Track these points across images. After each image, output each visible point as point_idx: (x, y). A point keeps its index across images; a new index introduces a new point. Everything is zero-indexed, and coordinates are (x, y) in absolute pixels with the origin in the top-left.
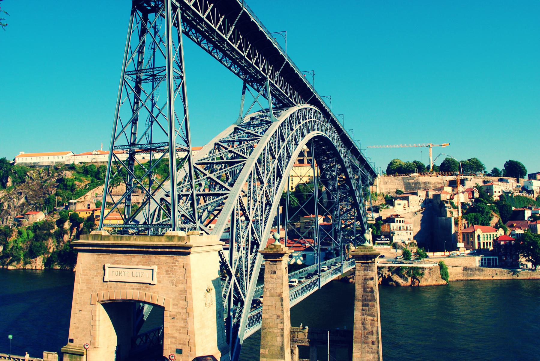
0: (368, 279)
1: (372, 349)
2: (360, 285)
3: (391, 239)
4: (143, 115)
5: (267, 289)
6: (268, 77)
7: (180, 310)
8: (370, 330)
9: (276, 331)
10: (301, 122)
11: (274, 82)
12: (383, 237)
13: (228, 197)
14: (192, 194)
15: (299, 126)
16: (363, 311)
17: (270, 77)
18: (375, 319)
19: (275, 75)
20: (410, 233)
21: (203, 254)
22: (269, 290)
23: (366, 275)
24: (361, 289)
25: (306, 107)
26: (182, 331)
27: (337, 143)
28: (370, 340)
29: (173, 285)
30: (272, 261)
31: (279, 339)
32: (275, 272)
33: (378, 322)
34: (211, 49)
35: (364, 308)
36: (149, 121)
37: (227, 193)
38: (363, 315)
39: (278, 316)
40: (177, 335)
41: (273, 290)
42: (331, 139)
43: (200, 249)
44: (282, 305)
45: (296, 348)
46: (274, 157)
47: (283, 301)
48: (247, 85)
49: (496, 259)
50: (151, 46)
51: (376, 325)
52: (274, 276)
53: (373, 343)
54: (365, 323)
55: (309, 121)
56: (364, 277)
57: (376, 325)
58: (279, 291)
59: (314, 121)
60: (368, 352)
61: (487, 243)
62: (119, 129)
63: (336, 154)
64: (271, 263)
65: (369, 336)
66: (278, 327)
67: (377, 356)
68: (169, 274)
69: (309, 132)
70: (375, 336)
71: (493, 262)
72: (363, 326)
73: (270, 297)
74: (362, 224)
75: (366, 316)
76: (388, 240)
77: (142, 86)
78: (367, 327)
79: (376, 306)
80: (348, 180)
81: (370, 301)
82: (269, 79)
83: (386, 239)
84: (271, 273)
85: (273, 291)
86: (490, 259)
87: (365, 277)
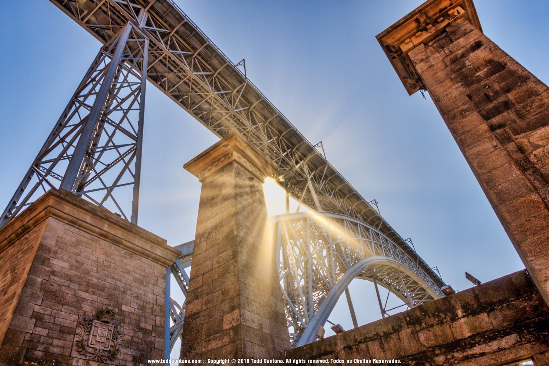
0: (463, 55)
16: (499, 131)
23: (451, 52)
24: (454, 87)
35: (495, 120)
38: (505, 140)
54: (532, 158)
56: (448, 60)
75: (521, 139)
87: (453, 55)
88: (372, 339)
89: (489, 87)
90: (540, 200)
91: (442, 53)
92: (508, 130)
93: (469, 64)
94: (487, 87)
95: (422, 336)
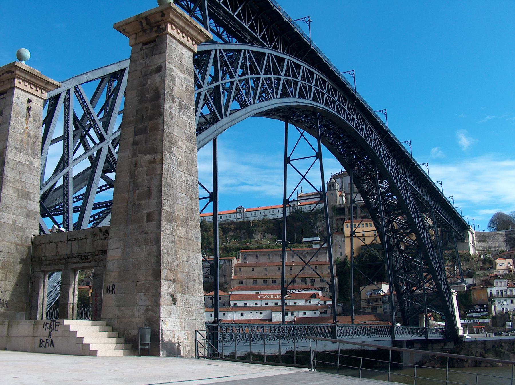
2: (136, 91)
3: (489, 310)
12: (477, 307)
16: (135, 147)
24: (136, 99)
33: (162, 163)
38: (134, 154)
60: (137, 242)
63: (375, 162)
65: (143, 202)
67: (154, 248)
72: (131, 180)
76: (484, 311)
79: (161, 128)
81: (150, 120)
83: (482, 310)
88: (75, 240)
89: (147, 110)
90: (127, 198)
91: (145, 62)
92: (138, 148)
93: (149, 83)
94: (146, 110)
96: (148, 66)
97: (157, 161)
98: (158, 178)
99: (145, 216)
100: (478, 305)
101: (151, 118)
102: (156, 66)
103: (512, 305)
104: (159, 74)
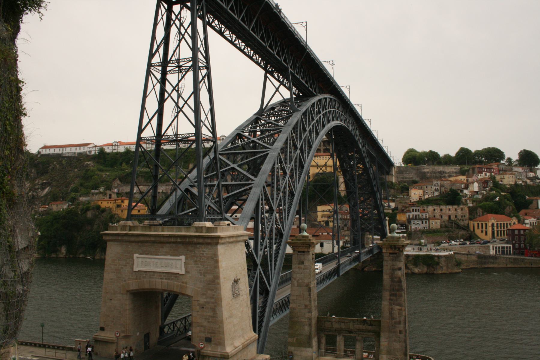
0: (396, 269)
1: (399, 338)
3: (407, 228)
4: (169, 106)
5: (295, 279)
6: (289, 67)
7: (208, 300)
8: (398, 320)
9: (304, 320)
10: (321, 112)
11: (294, 72)
13: (252, 187)
14: (218, 184)
15: (320, 115)
16: (391, 301)
17: (291, 68)
18: (403, 308)
19: (296, 66)
20: (426, 222)
21: (230, 245)
22: (297, 280)
23: (394, 265)
25: (326, 96)
26: (210, 320)
27: (355, 133)
28: (398, 329)
29: (201, 275)
30: (299, 252)
31: (307, 328)
32: (303, 263)
34: (234, 39)
35: (392, 297)
36: (175, 112)
37: (251, 184)
38: (390, 304)
39: (306, 306)
40: (205, 324)
41: (301, 280)
42: (350, 129)
43: (228, 240)
44: (310, 295)
45: (323, 337)
46: (296, 148)
47: (310, 291)
48: (268, 75)
49: (510, 247)
50: (176, 37)
51: (404, 314)
52: (302, 266)
53: (400, 332)
55: (329, 111)
57: (404, 314)
58: (306, 281)
59: (333, 111)
60: (395, 341)
61: (501, 231)
62: (145, 121)
63: (354, 143)
64: (299, 254)
66: (306, 316)
67: (404, 345)
68: (198, 264)
69: (329, 122)
70: (402, 326)
71: (507, 251)
73: (298, 287)
74: (379, 213)
76: (404, 229)
77: (168, 77)
78: (395, 316)
80: (365, 170)
81: (398, 291)
82: (290, 69)
83: (402, 228)
84: (299, 264)
85: (300, 281)
86: (504, 247)
95: (355, 326)
96: (394, 265)
97: (403, 310)
98: (404, 317)
99: (399, 331)
100: (400, 224)
101: (398, 290)
102: (398, 267)
103: (423, 225)
104: (401, 271)
